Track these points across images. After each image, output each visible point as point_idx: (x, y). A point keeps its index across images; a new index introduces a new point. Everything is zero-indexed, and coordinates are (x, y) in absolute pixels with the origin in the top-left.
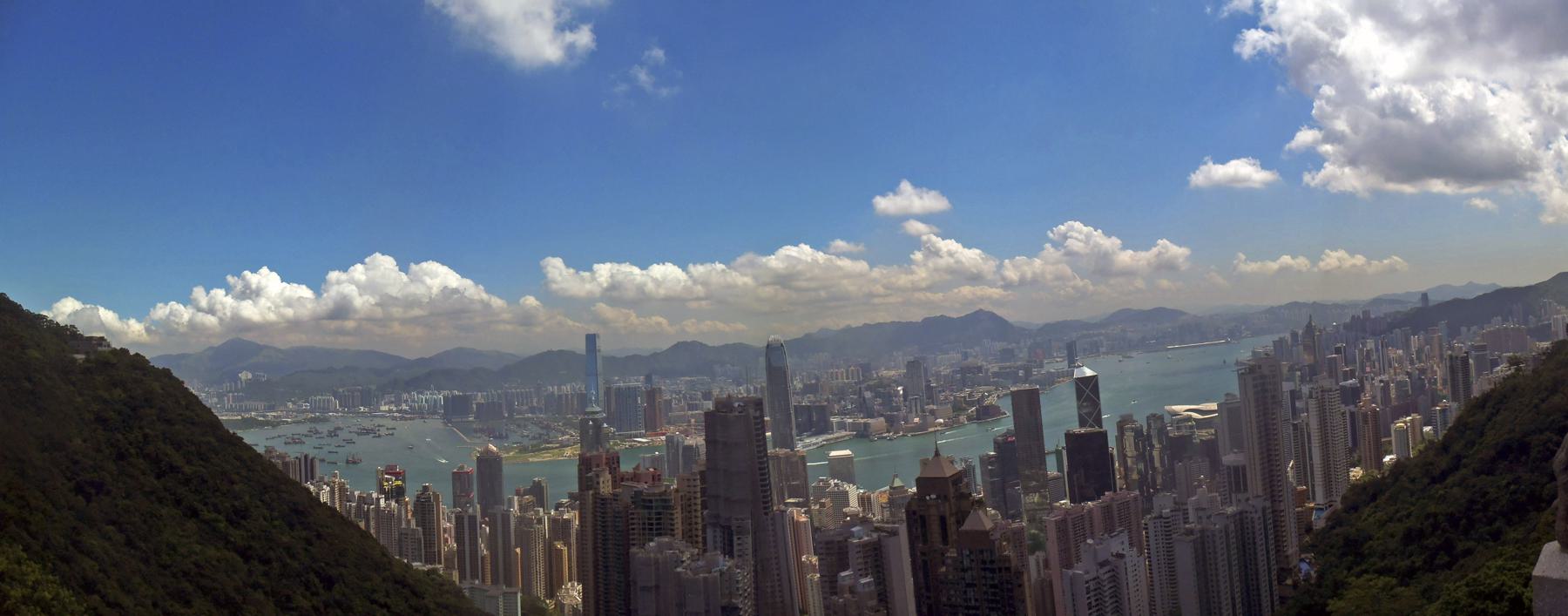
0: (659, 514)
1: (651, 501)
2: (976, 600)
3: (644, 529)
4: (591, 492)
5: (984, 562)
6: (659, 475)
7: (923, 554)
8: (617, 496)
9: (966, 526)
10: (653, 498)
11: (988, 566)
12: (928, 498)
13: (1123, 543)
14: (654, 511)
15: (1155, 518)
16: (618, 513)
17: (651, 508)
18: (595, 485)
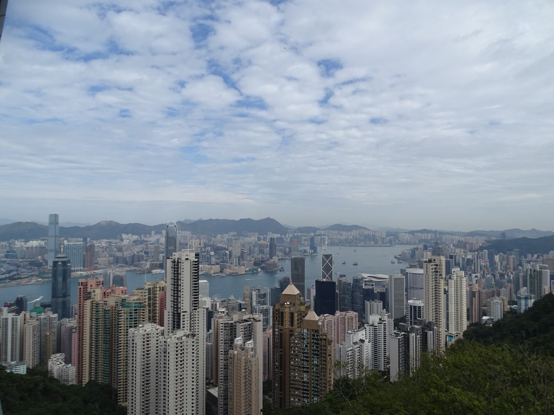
0: (136, 310)
4: (91, 300)
6: (125, 290)
7: (281, 330)
8: (106, 301)
9: (307, 318)
12: (285, 304)
13: (363, 335)
16: (107, 311)
18: (93, 296)
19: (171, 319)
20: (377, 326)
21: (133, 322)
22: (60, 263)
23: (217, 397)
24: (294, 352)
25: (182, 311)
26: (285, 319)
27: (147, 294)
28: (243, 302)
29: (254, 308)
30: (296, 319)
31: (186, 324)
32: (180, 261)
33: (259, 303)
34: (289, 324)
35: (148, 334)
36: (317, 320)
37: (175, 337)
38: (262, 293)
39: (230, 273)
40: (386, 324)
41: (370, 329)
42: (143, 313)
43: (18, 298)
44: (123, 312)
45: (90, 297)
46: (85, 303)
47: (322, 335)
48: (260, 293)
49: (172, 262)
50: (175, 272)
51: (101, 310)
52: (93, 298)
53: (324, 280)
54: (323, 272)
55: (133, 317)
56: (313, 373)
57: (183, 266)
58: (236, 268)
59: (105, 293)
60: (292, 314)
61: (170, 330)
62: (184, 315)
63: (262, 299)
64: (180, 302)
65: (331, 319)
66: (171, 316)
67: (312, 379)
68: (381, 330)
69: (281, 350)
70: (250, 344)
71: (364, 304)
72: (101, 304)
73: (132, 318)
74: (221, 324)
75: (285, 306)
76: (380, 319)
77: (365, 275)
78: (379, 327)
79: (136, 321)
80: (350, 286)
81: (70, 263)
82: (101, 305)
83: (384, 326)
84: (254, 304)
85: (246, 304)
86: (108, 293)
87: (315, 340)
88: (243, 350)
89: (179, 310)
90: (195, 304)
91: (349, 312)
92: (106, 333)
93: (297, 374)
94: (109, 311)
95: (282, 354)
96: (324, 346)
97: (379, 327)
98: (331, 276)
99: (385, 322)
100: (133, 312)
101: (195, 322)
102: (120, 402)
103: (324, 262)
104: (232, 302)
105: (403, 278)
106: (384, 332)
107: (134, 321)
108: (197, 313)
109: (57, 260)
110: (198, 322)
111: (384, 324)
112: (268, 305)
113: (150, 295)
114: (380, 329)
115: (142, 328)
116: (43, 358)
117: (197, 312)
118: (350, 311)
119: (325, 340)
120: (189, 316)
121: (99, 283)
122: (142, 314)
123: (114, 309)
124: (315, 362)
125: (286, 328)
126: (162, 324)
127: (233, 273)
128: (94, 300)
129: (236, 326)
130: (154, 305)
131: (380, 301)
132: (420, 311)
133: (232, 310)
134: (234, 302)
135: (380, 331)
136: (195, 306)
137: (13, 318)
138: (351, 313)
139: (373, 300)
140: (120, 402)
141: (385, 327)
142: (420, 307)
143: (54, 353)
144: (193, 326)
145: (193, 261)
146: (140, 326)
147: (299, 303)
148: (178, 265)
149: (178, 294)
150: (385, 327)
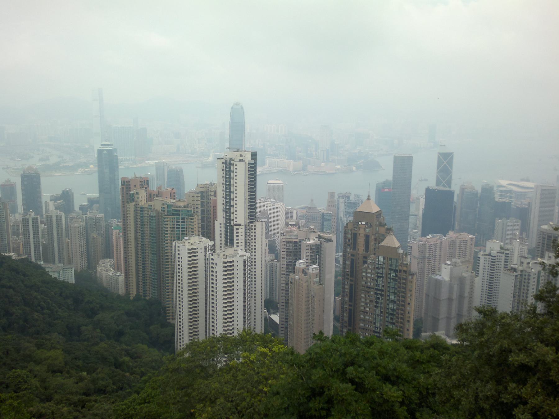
1: (179, 210)
2: (383, 286)
3: (174, 228)
4: (134, 203)
5: (391, 265)
6: (174, 193)
7: (352, 255)
8: (151, 206)
10: (180, 209)
11: (394, 267)
12: (360, 223)
13: (468, 267)
14: (180, 217)
15: (486, 255)
16: (152, 217)
17: (178, 215)
18: (136, 199)
19: (223, 232)
20: (495, 257)
22: (105, 152)
23: (278, 323)
25: (235, 223)
26: (359, 243)
27: (199, 198)
30: (372, 243)
31: (240, 239)
32: (232, 162)
34: (364, 248)
35: (195, 249)
36: (397, 246)
37: (224, 255)
38: (352, 201)
39: (316, 172)
40: (508, 254)
41: (486, 259)
42: (192, 222)
43: (63, 191)
44: (168, 219)
45: (133, 199)
46: (128, 206)
47: (401, 266)
48: (350, 201)
49: (223, 163)
50: (227, 176)
51: (146, 215)
52: (136, 201)
53: (439, 188)
54: (437, 177)
55: (181, 227)
56: (388, 310)
57: (236, 169)
58: (323, 164)
59: (150, 195)
60: (367, 237)
61: (223, 245)
62: (237, 229)
64: (233, 213)
65: (436, 243)
66: (223, 229)
67: (387, 317)
68: (501, 262)
70: (314, 269)
72: (146, 208)
73: (179, 228)
74: (284, 242)
75: (360, 226)
76: (501, 248)
78: (498, 257)
79: (185, 231)
81: (117, 153)
82: (146, 209)
83: (506, 256)
84: (341, 215)
86: (154, 195)
87: (392, 271)
88: (306, 276)
89: (232, 222)
90: (252, 216)
92: (153, 243)
93: (368, 309)
94: (154, 217)
97: (498, 257)
98: (449, 183)
99: (507, 252)
100: (180, 220)
101: (252, 237)
102: (169, 319)
103: (440, 162)
106: (505, 265)
107: (182, 231)
108: (253, 228)
109: (102, 148)
110: (255, 237)
111: (506, 254)
113: (204, 199)
114: (500, 260)
115: (189, 241)
116: (91, 263)
117: (253, 226)
118: (464, 233)
119: (405, 272)
120: (243, 230)
121: (143, 183)
122: (190, 223)
123: (160, 215)
124: (392, 297)
125: (358, 253)
126: (212, 238)
128: (137, 203)
129: (300, 245)
130: (208, 213)
135: (500, 263)
136: (251, 219)
137: (57, 217)
140: (169, 319)
141: (507, 258)
143: (103, 258)
144: (249, 243)
145: (249, 164)
146: (186, 238)
147: (378, 223)
148: (230, 168)
149: (230, 203)
150: (507, 258)
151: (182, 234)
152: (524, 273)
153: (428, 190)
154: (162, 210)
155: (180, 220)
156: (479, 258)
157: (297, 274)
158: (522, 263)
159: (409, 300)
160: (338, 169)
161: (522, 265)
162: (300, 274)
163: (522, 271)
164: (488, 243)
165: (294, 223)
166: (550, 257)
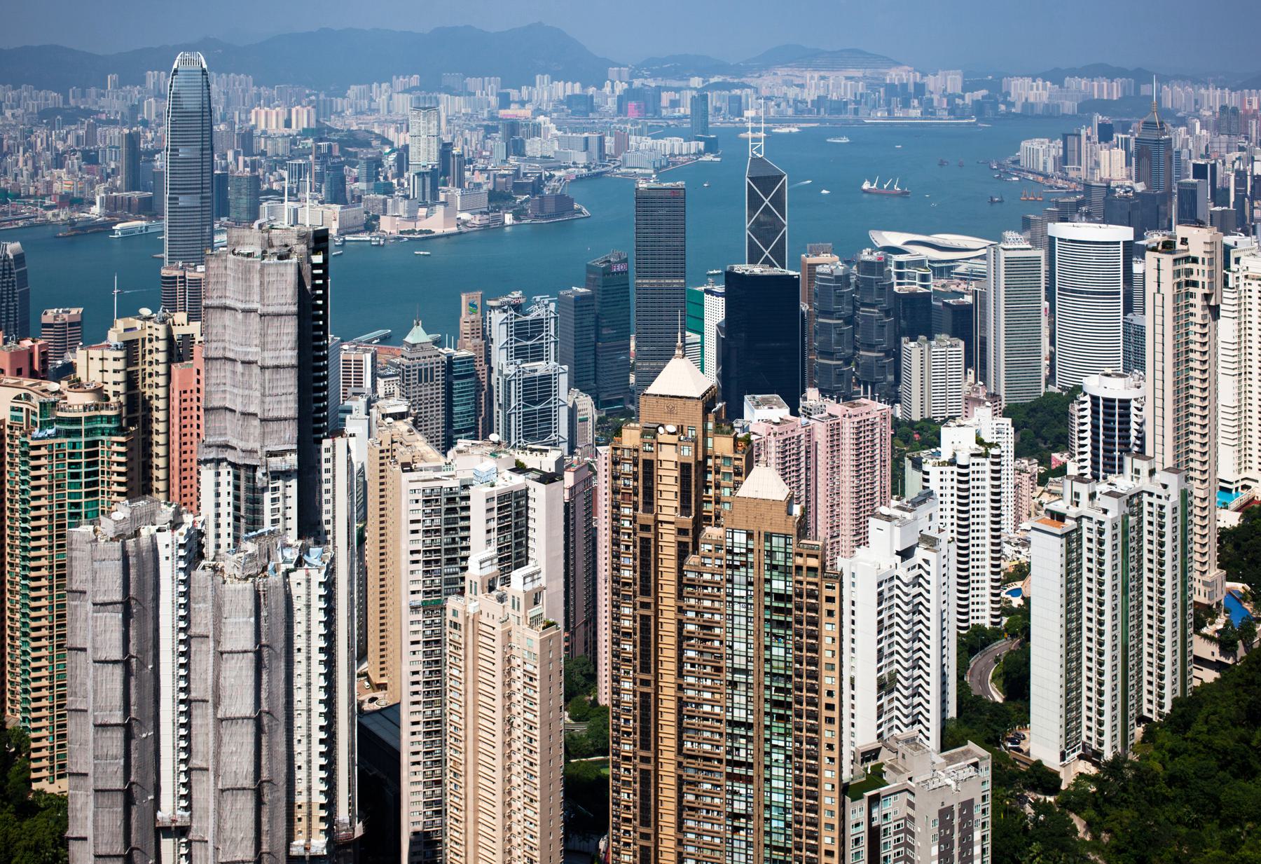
7: (645, 528)
15: (943, 464)
20: (967, 467)
21: (83, 490)
24: (697, 613)
27: (120, 365)
28: (464, 353)
29: (501, 372)
33: (520, 353)
38: (529, 318)
40: (999, 456)
41: (943, 476)
44: (43, 451)
58: (422, 211)
63: (529, 339)
69: (646, 600)
70: (528, 579)
71: (895, 354)
76: (980, 441)
77: (895, 239)
78: (975, 468)
80: (849, 285)
84: (500, 358)
85: (470, 360)
91: (859, 405)
95: (648, 617)
96: (811, 594)
97: (975, 468)
99: (994, 451)
100: (83, 450)
104: (420, 355)
105: (1038, 259)
107: (88, 485)
111: (993, 456)
112: (552, 363)
127: (413, 231)
131: (956, 340)
132: (1125, 416)
133: (420, 381)
134: (427, 354)
135: (979, 483)
138: (864, 410)
139: (930, 338)
142: (1128, 401)
151: (88, 495)
152: (1085, 523)
153: (732, 279)
154: (13, 417)
155: (83, 450)
156: (927, 473)
157: (472, 596)
158: (1077, 495)
159: (829, 654)
160: (465, 223)
161: (1077, 504)
162: (480, 595)
163: (1078, 519)
164: (944, 430)
165: (403, 409)
166: (1137, 471)
